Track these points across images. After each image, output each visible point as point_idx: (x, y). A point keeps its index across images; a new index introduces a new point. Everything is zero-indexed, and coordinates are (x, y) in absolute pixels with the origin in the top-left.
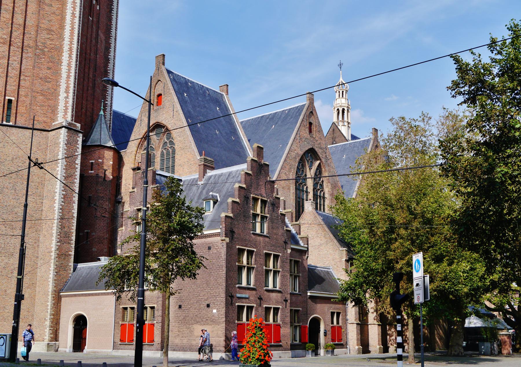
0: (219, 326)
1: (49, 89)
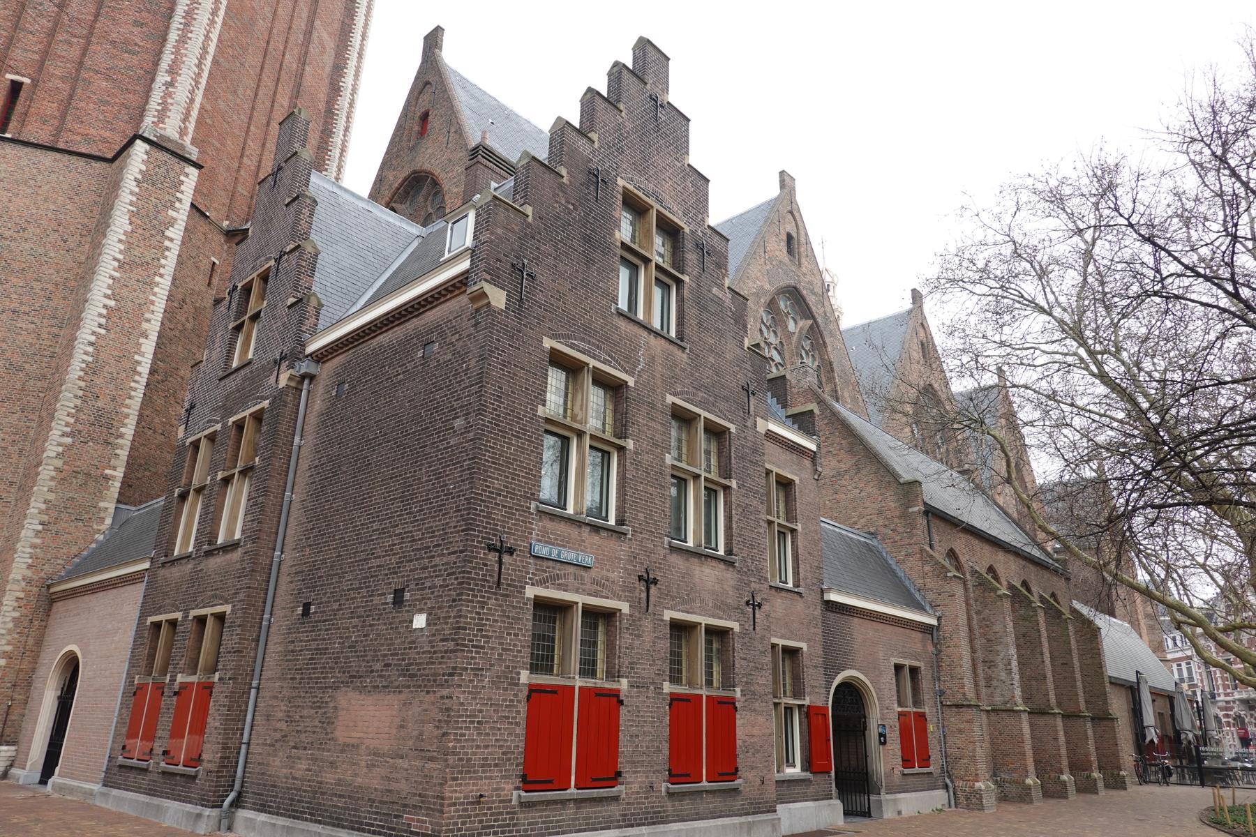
0: (431, 697)
1: (129, 68)
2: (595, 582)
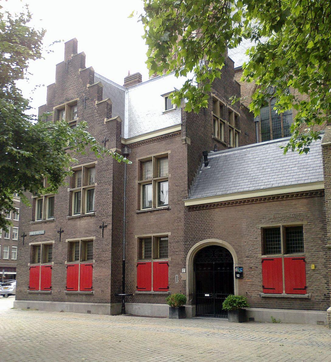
2: (46, 237)
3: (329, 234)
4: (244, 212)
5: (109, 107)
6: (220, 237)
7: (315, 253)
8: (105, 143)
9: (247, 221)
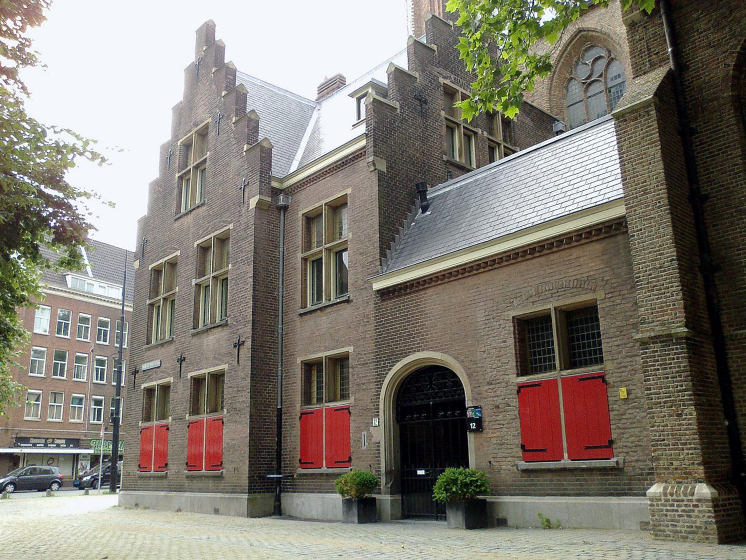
3: (643, 309)
4: (480, 289)
5: (252, 124)
6: (436, 347)
7: (625, 360)
8: (244, 190)
9: (486, 307)
